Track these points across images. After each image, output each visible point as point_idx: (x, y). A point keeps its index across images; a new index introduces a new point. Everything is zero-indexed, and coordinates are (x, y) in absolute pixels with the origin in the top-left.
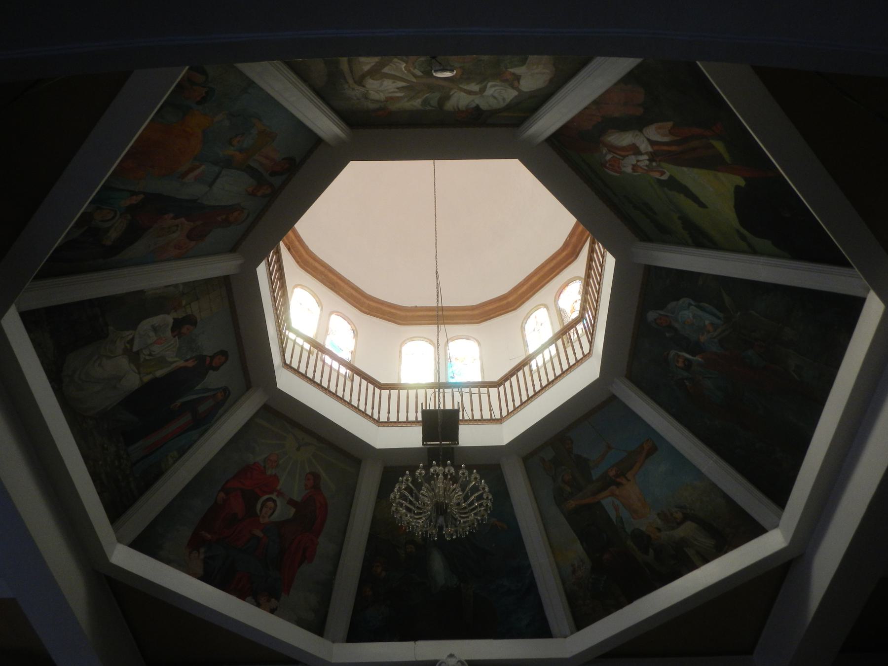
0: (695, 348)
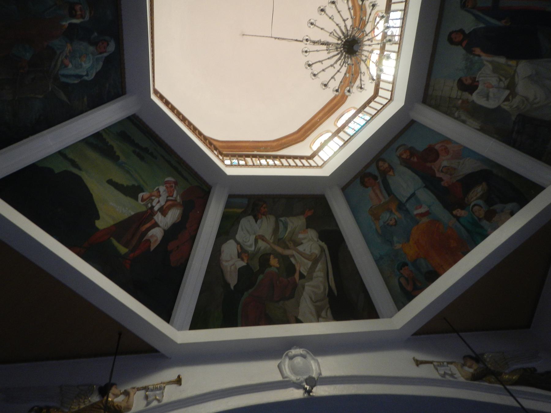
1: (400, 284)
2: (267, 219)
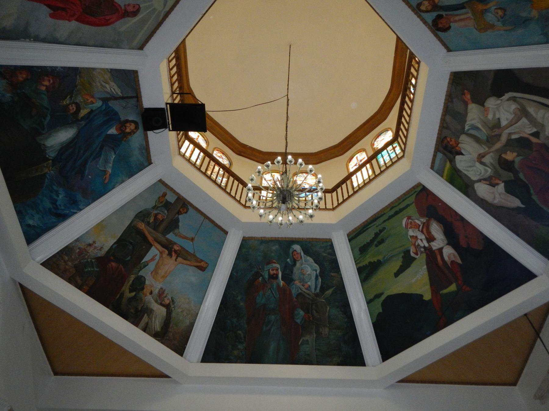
0: (288, 279)
2: (465, 143)
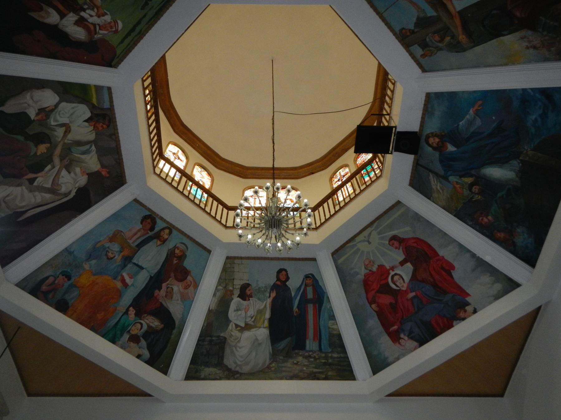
1: (47, 278)
2: (90, 132)
